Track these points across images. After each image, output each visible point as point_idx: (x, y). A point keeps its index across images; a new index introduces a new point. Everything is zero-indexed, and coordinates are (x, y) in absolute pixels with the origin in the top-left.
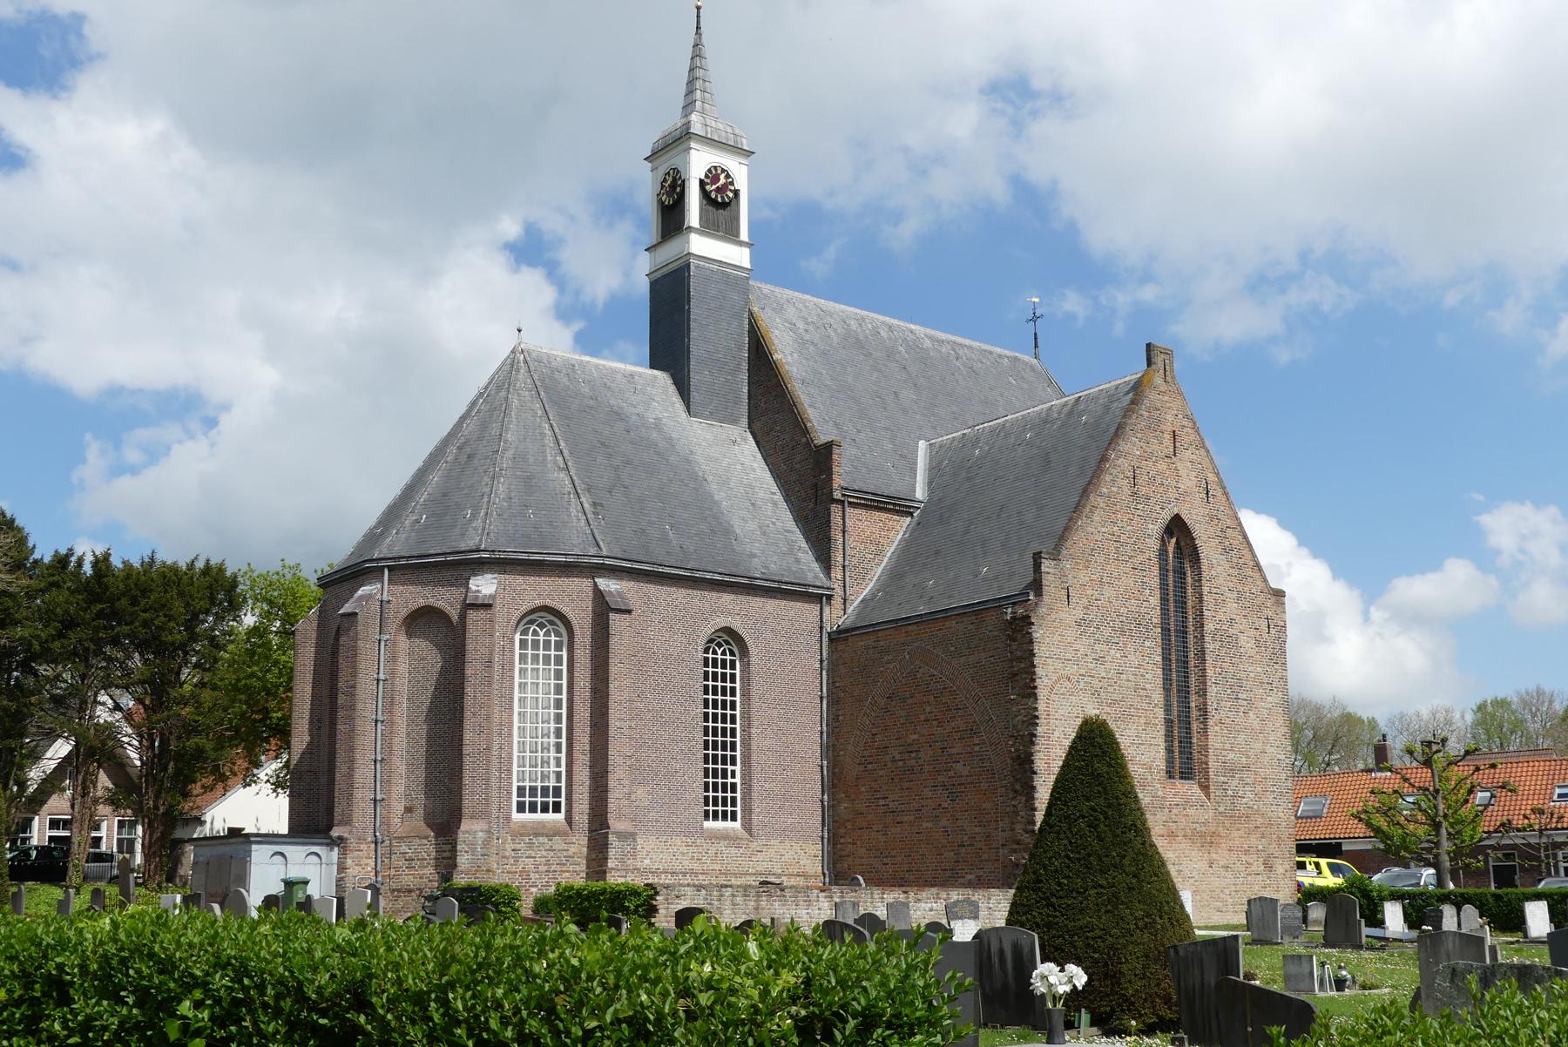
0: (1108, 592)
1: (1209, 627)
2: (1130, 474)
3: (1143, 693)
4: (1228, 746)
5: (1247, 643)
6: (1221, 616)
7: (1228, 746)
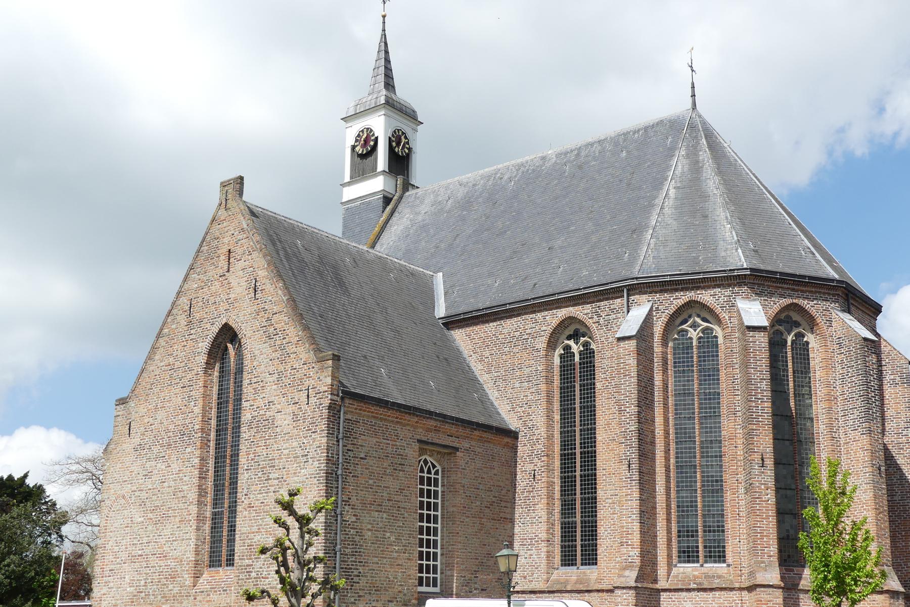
0: (161, 415)
1: (246, 416)
2: (187, 308)
3: (180, 494)
4: (255, 529)
5: (284, 422)
6: (260, 402)
7: (255, 529)
